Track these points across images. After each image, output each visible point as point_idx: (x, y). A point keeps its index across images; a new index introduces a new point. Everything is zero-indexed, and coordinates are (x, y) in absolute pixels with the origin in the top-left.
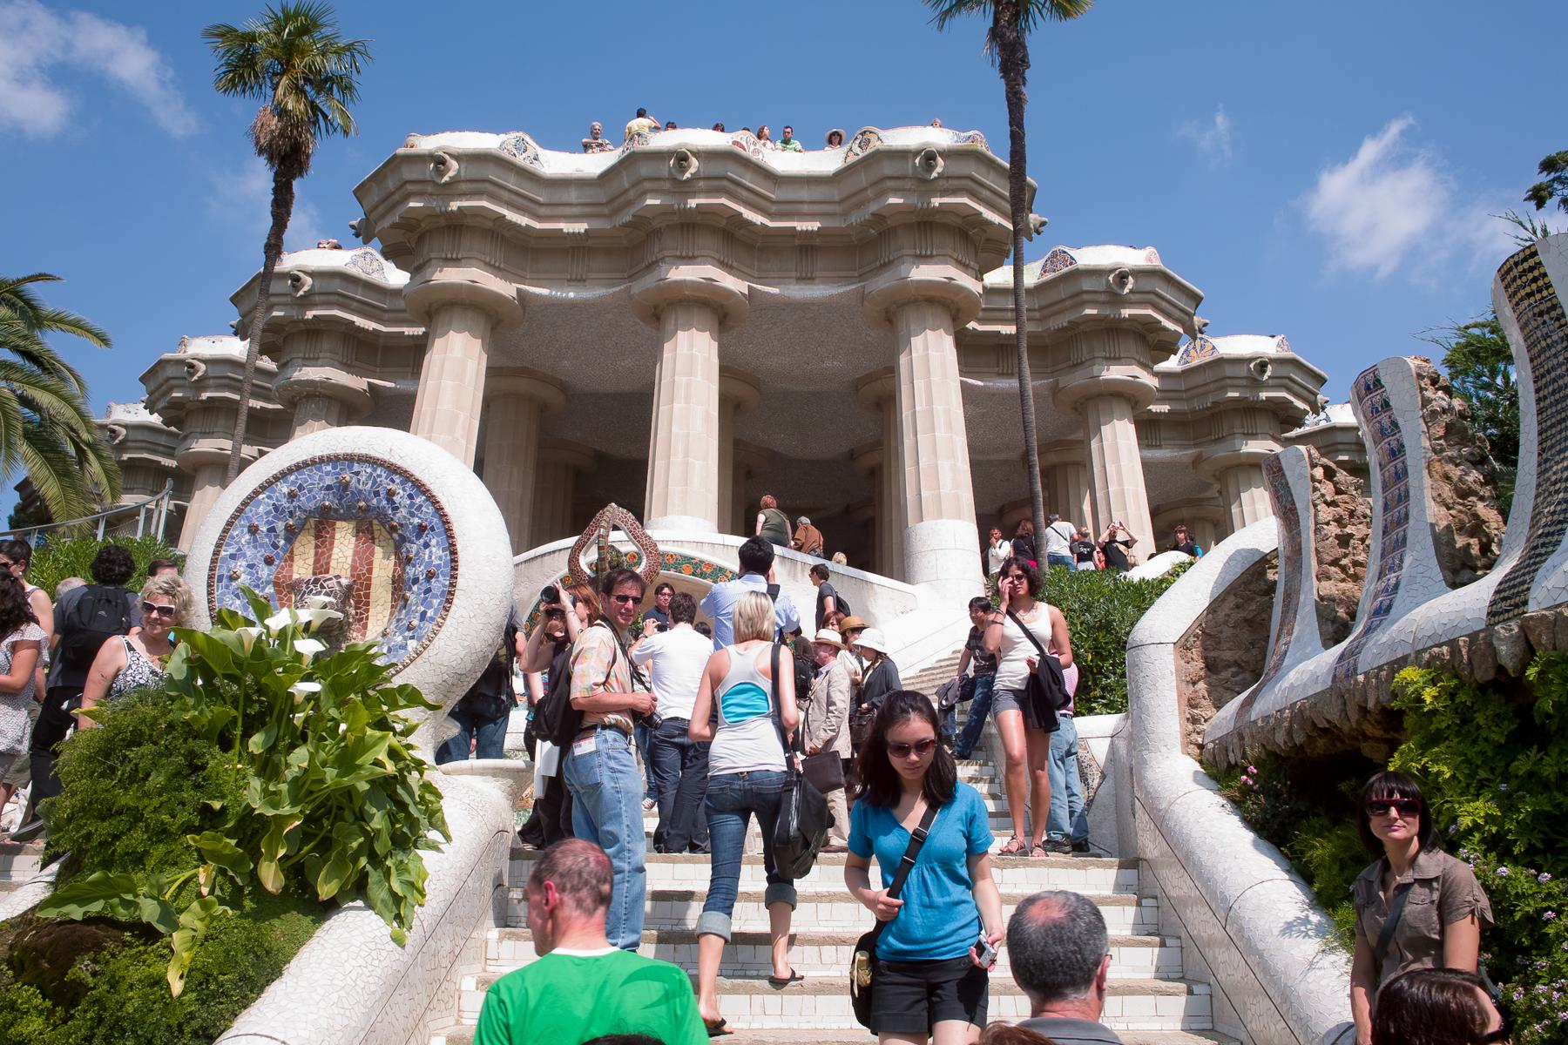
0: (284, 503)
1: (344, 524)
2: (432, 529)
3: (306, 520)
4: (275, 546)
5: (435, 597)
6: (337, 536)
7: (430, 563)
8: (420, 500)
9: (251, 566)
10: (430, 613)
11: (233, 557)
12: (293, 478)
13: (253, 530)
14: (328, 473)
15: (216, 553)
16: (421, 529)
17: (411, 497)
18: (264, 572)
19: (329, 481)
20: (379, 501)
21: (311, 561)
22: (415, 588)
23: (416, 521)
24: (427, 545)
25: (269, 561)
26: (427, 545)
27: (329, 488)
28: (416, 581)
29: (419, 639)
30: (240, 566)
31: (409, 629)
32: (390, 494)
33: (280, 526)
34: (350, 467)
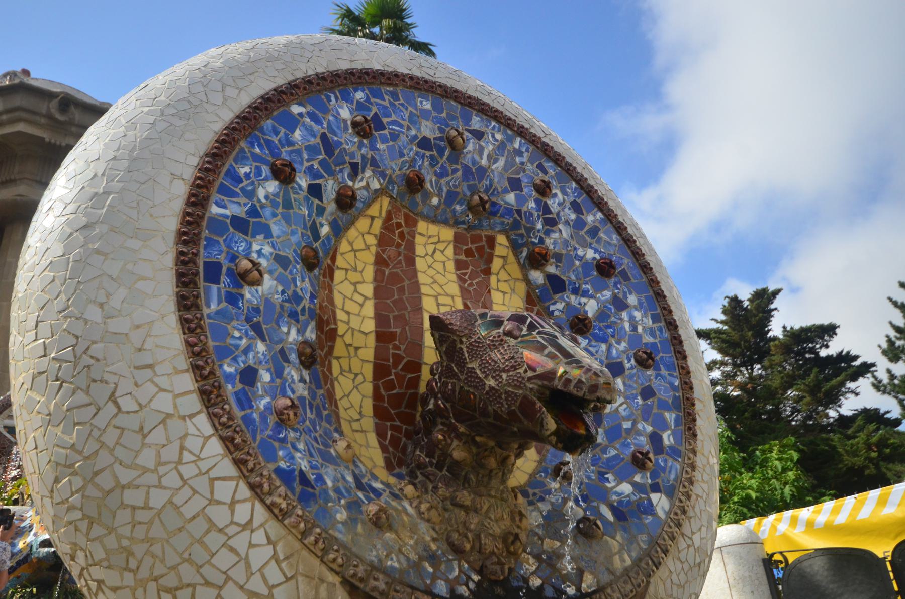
0: (349, 141)
1: (433, 229)
2: (626, 278)
3: (378, 194)
4: (315, 230)
5: (663, 405)
6: (419, 250)
7: (635, 338)
8: (593, 218)
9: (281, 261)
10: (667, 439)
11: (240, 224)
12: (360, 96)
13: (283, 174)
14: (425, 114)
15: (197, 200)
16: (605, 269)
17: (575, 206)
18: (304, 286)
19: (428, 130)
20: (521, 200)
21: (368, 289)
22: (619, 383)
23: (590, 254)
24: (620, 304)
25: (310, 263)
26: (620, 304)
27: (424, 143)
28: (617, 369)
29: (670, 493)
30: (261, 249)
31: (639, 461)
32: (543, 190)
33: (330, 188)
34: (467, 120)
